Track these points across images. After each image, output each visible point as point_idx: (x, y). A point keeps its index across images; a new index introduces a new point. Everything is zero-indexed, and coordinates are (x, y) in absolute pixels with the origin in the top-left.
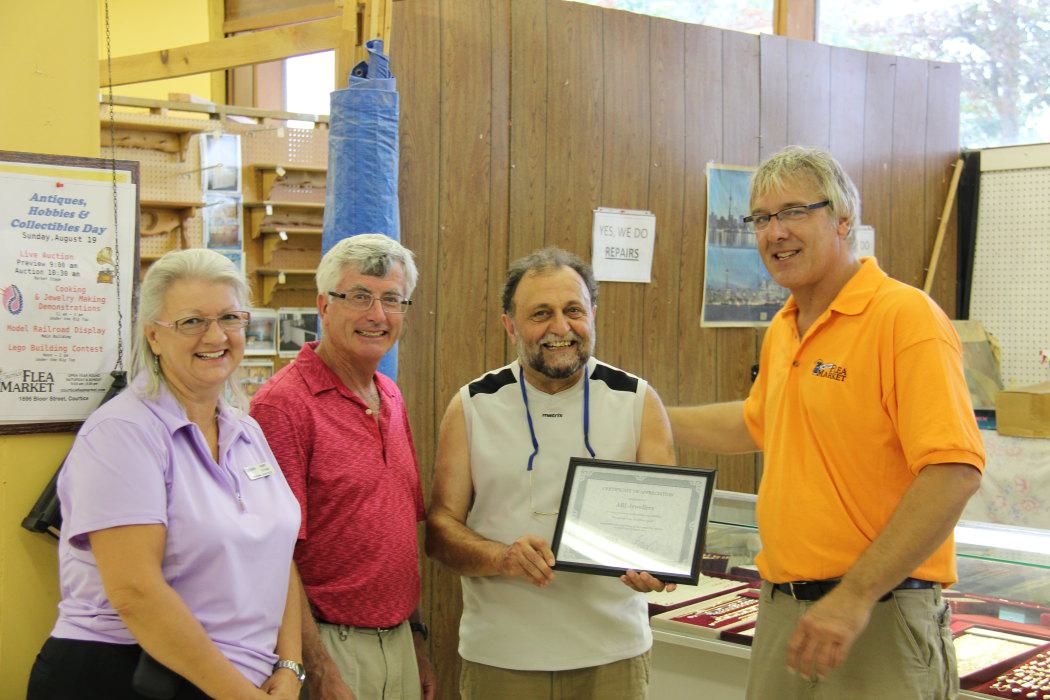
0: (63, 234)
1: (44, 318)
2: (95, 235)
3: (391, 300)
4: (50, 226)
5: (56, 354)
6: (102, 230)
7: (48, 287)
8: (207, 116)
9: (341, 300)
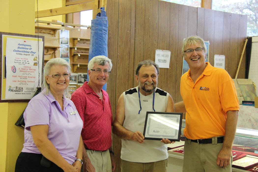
1: (21, 74)
4: (22, 51)
7: (22, 66)
8: (61, 26)
9: (94, 71)
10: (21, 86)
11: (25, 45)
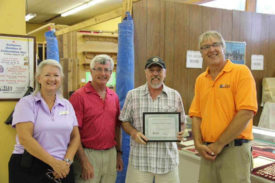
0: (15, 53)
1: (9, 74)
2: (23, 54)
3: (107, 70)
5: (13, 82)
6: (25, 53)
7: (11, 66)
8: (111, 34)
9: (94, 70)
10: (10, 85)
11: (15, 45)
